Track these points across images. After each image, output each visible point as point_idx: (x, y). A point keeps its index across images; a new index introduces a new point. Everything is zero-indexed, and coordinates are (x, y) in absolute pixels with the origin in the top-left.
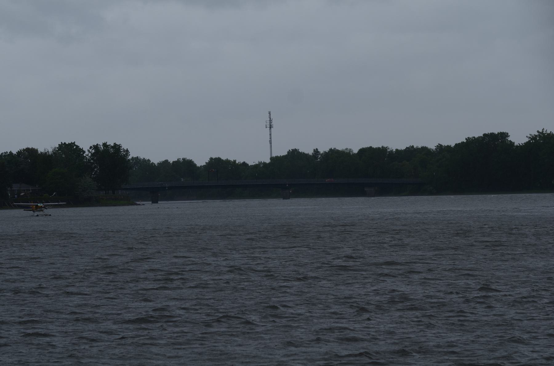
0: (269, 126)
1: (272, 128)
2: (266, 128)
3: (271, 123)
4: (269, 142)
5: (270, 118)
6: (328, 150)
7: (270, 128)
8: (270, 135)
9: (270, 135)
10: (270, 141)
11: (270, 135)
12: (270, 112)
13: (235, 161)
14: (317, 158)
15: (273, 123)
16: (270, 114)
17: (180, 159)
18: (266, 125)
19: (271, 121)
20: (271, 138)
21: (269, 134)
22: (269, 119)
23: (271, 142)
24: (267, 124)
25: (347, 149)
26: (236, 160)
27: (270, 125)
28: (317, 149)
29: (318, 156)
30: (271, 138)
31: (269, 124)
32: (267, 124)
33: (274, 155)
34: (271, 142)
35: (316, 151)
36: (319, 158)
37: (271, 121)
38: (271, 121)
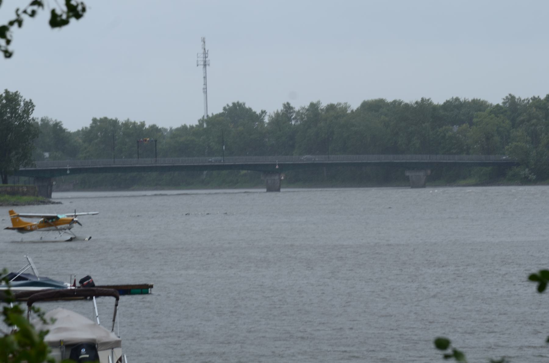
0: (202, 63)
1: (207, 67)
2: (198, 65)
3: (206, 57)
4: (202, 91)
5: (205, 49)
6: (309, 104)
7: (205, 65)
8: (205, 78)
9: (204, 77)
10: (204, 89)
11: (205, 78)
12: (204, 39)
13: (143, 124)
14: (290, 119)
15: (210, 58)
16: (204, 42)
17: (38, 119)
18: (197, 61)
19: (205, 54)
20: (205, 84)
22: (202, 51)
23: (205, 91)
24: (199, 59)
26: (144, 122)
27: (205, 62)
28: (288, 104)
29: (292, 116)
30: (205, 84)
31: (202, 59)
32: (199, 59)
34: (205, 91)
35: (288, 107)
36: (294, 119)
37: (205, 54)
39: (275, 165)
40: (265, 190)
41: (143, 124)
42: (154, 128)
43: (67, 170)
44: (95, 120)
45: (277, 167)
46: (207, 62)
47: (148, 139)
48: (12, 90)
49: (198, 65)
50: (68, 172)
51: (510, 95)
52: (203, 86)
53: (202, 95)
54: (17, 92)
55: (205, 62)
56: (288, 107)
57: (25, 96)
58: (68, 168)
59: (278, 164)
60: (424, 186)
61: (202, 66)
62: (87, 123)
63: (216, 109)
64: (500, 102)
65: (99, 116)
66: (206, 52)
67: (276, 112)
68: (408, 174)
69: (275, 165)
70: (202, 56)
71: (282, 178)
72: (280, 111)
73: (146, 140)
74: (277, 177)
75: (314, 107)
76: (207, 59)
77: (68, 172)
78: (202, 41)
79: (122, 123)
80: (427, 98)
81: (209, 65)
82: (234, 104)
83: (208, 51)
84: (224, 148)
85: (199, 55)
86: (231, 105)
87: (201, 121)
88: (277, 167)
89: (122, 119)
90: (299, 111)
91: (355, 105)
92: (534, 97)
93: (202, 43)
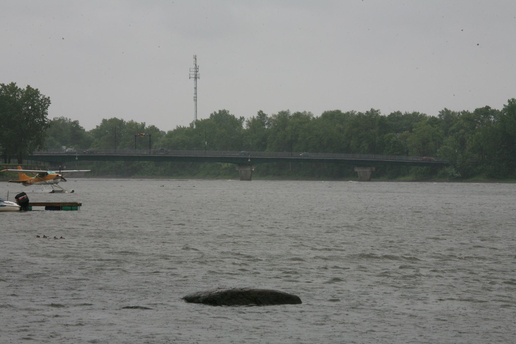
0: (194, 76)
2: (190, 78)
3: (197, 72)
4: (193, 99)
5: (196, 65)
7: (196, 78)
8: (196, 88)
11: (196, 88)
12: (196, 56)
13: (143, 125)
14: (263, 124)
15: (200, 72)
16: (196, 59)
18: (190, 74)
19: (196, 69)
20: (196, 94)
21: (194, 86)
23: (196, 100)
25: (305, 112)
26: (145, 123)
27: (196, 75)
28: (261, 111)
30: (196, 94)
33: (199, 119)
34: (196, 100)
35: (262, 115)
36: (266, 124)
37: (196, 69)
39: (248, 159)
41: (143, 125)
42: (153, 129)
43: (75, 156)
44: (104, 121)
45: (249, 160)
46: (198, 75)
47: (144, 134)
49: (190, 78)
50: (77, 158)
51: (445, 109)
53: (193, 103)
55: (196, 75)
56: (262, 115)
59: (250, 158)
60: (369, 180)
61: (194, 79)
62: (99, 123)
63: (204, 115)
64: (436, 115)
66: (197, 67)
67: (252, 117)
68: (356, 170)
69: (248, 159)
70: (194, 70)
71: (253, 170)
72: (255, 117)
73: (142, 135)
74: (248, 169)
76: (197, 73)
77: (77, 158)
79: (127, 123)
80: (376, 110)
82: (220, 111)
83: (198, 66)
84: (206, 144)
85: (191, 70)
86: (218, 112)
87: (191, 125)
88: (249, 160)
89: (127, 120)
91: (317, 113)
92: (464, 111)
93: (194, 59)
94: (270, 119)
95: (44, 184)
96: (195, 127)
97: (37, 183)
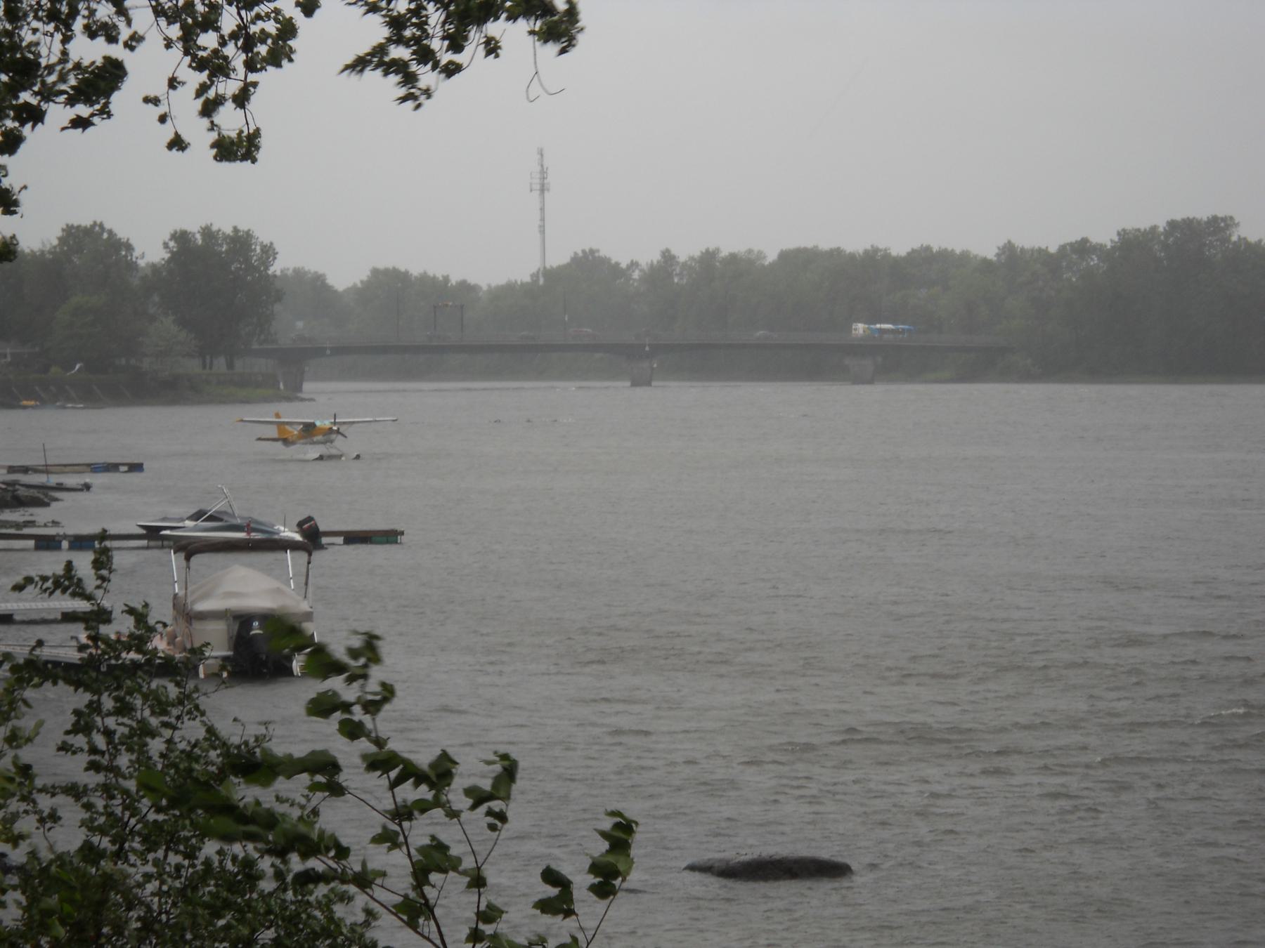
0: (538, 187)
1: (546, 192)
2: (531, 191)
3: (544, 178)
5: (542, 166)
7: (543, 190)
8: (542, 209)
9: (541, 209)
10: (540, 226)
11: (542, 209)
12: (542, 150)
13: (446, 279)
15: (550, 179)
16: (542, 155)
17: (288, 269)
18: (531, 184)
19: (543, 173)
20: (543, 219)
22: (539, 168)
25: (750, 251)
28: (668, 251)
29: (674, 270)
30: (543, 219)
31: (538, 181)
33: (548, 266)
35: (668, 257)
36: (676, 275)
37: (543, 173)
38: (544, 172)
39: (645, 347)
40: (628, 384)
41: (446, 279)
45: (647, 349)
47: (450, 304)
48: (243, 227)
50: (328, 352)
52: (539, 223)
54: (249, 230)
56: (668, 257)
57: (263, 235)
58: (328, 346)
59: (649, 345)
60: (871, 381)
61: (538, 192)
63: (559, 257)
65: (381, 265)
66: (545, 170)
67: (650, 262)
70: (538, 176)
71: (655, 366)
72: (655, 262)
73: (447, 305)
75: (709, 257)
76: (545, 181)
77: (328, 352)
78: (538, 153)
79: (416, 277)
81: (548, 190)
83: (547, 168)
84: (566, 319)
87: (535, 276)
88: (647, 349)
89: (415, 271)
90: (686, 262)
93: (539, 156)
94: (684, 265)
95: (311, 444)
96: (541, 281)
97: (302, 441)
